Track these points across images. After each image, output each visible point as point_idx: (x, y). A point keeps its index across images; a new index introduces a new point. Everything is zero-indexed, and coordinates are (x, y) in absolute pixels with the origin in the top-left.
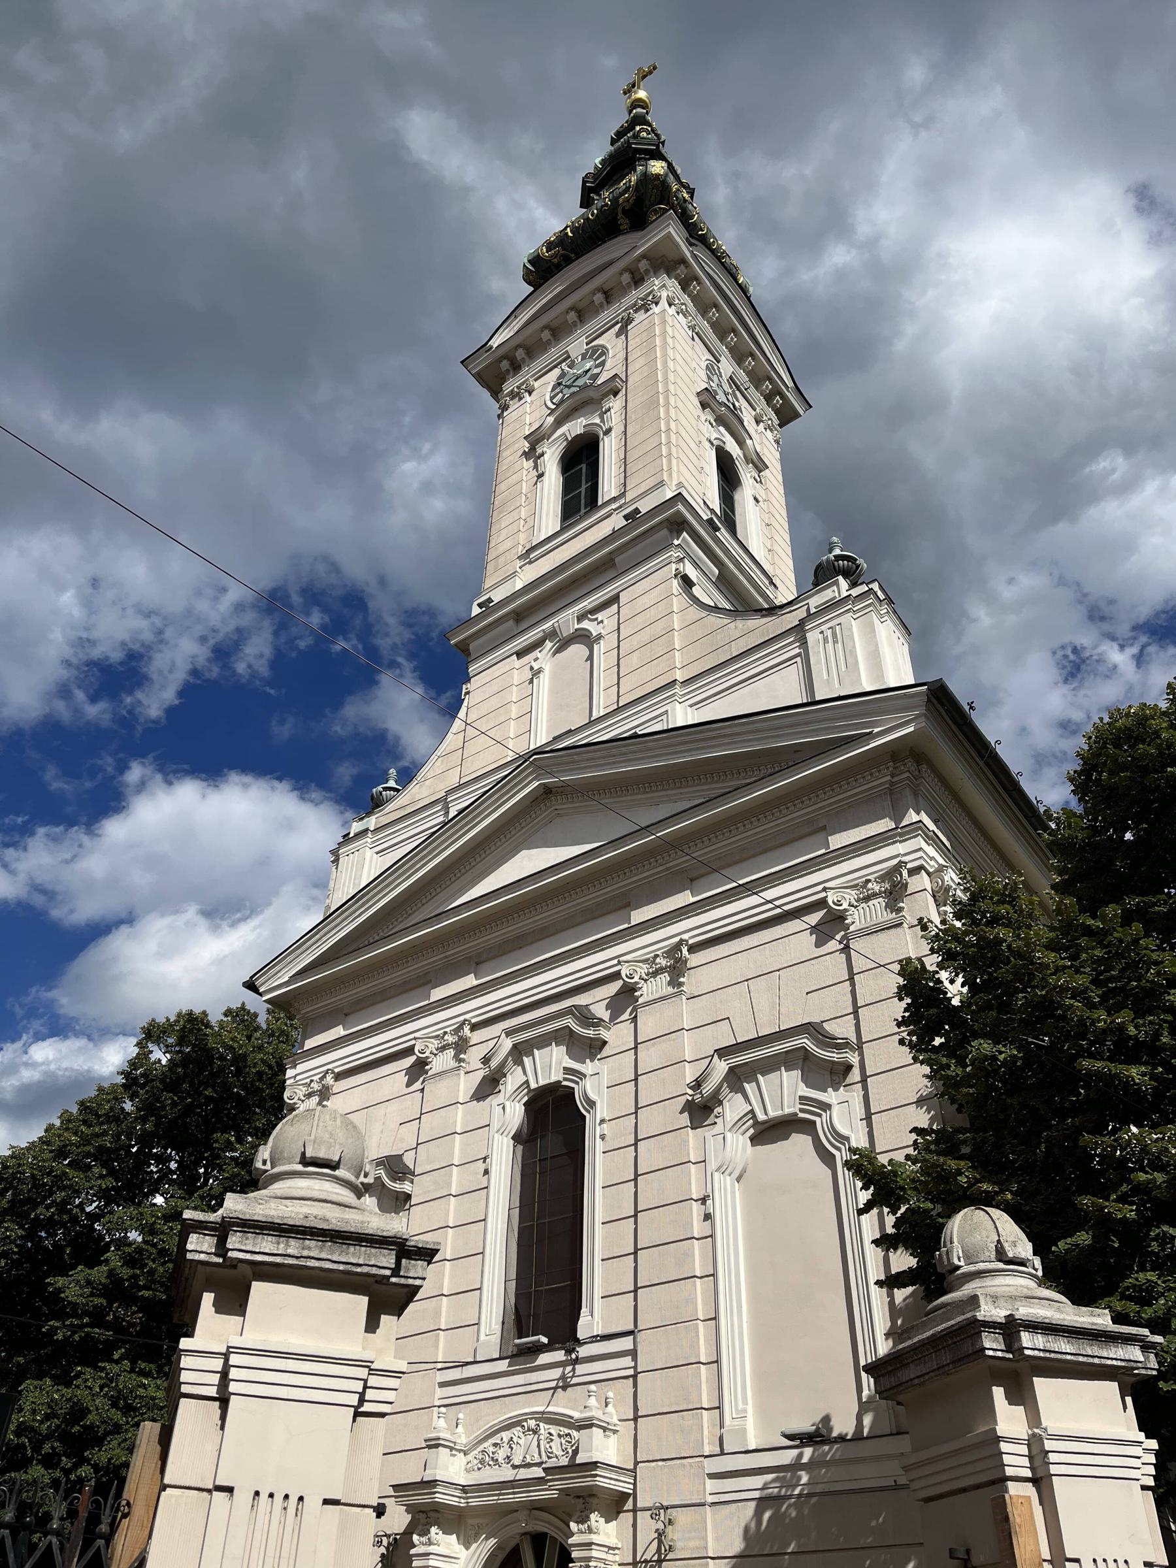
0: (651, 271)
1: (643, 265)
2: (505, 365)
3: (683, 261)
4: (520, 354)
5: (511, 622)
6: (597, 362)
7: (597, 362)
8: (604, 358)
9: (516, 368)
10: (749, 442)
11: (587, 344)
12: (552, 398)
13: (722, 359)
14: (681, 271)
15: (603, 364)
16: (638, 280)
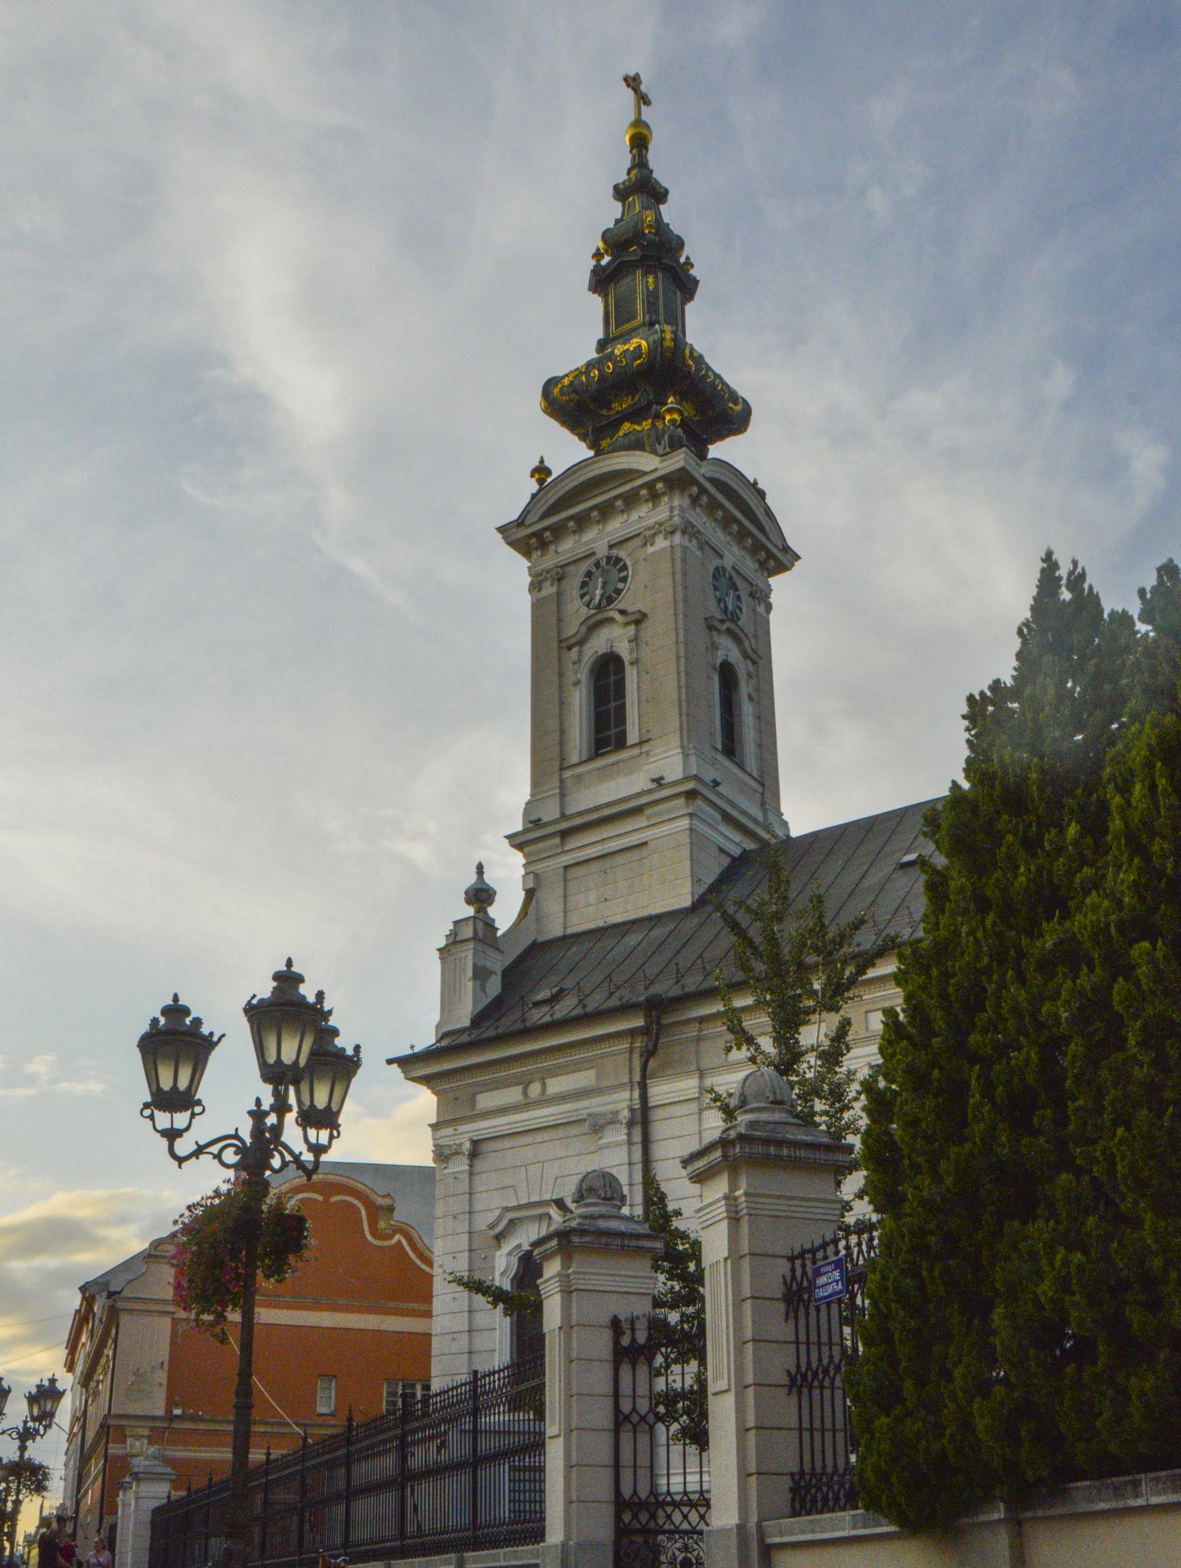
0: (668, 492)
1: (660, 485)
2: (534, 540)
3: (695, 482)
4: (547, 534)
5: (557, 840)
6: (622, 575)
7: (622, 575)
8: (624, 574)
9: (543, 545)
10: (747, 644)
11: (611, 547)
12: (582, 596)
13: (727, 554)
14: (695, 489)
15: (624, 580)
16: (654, 497)
